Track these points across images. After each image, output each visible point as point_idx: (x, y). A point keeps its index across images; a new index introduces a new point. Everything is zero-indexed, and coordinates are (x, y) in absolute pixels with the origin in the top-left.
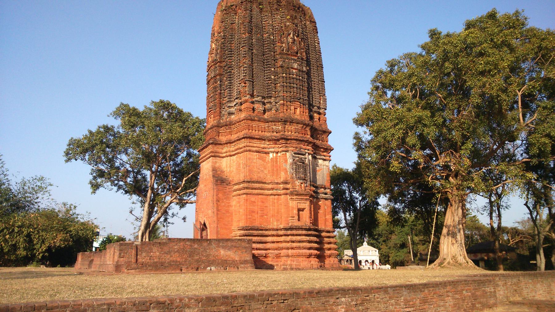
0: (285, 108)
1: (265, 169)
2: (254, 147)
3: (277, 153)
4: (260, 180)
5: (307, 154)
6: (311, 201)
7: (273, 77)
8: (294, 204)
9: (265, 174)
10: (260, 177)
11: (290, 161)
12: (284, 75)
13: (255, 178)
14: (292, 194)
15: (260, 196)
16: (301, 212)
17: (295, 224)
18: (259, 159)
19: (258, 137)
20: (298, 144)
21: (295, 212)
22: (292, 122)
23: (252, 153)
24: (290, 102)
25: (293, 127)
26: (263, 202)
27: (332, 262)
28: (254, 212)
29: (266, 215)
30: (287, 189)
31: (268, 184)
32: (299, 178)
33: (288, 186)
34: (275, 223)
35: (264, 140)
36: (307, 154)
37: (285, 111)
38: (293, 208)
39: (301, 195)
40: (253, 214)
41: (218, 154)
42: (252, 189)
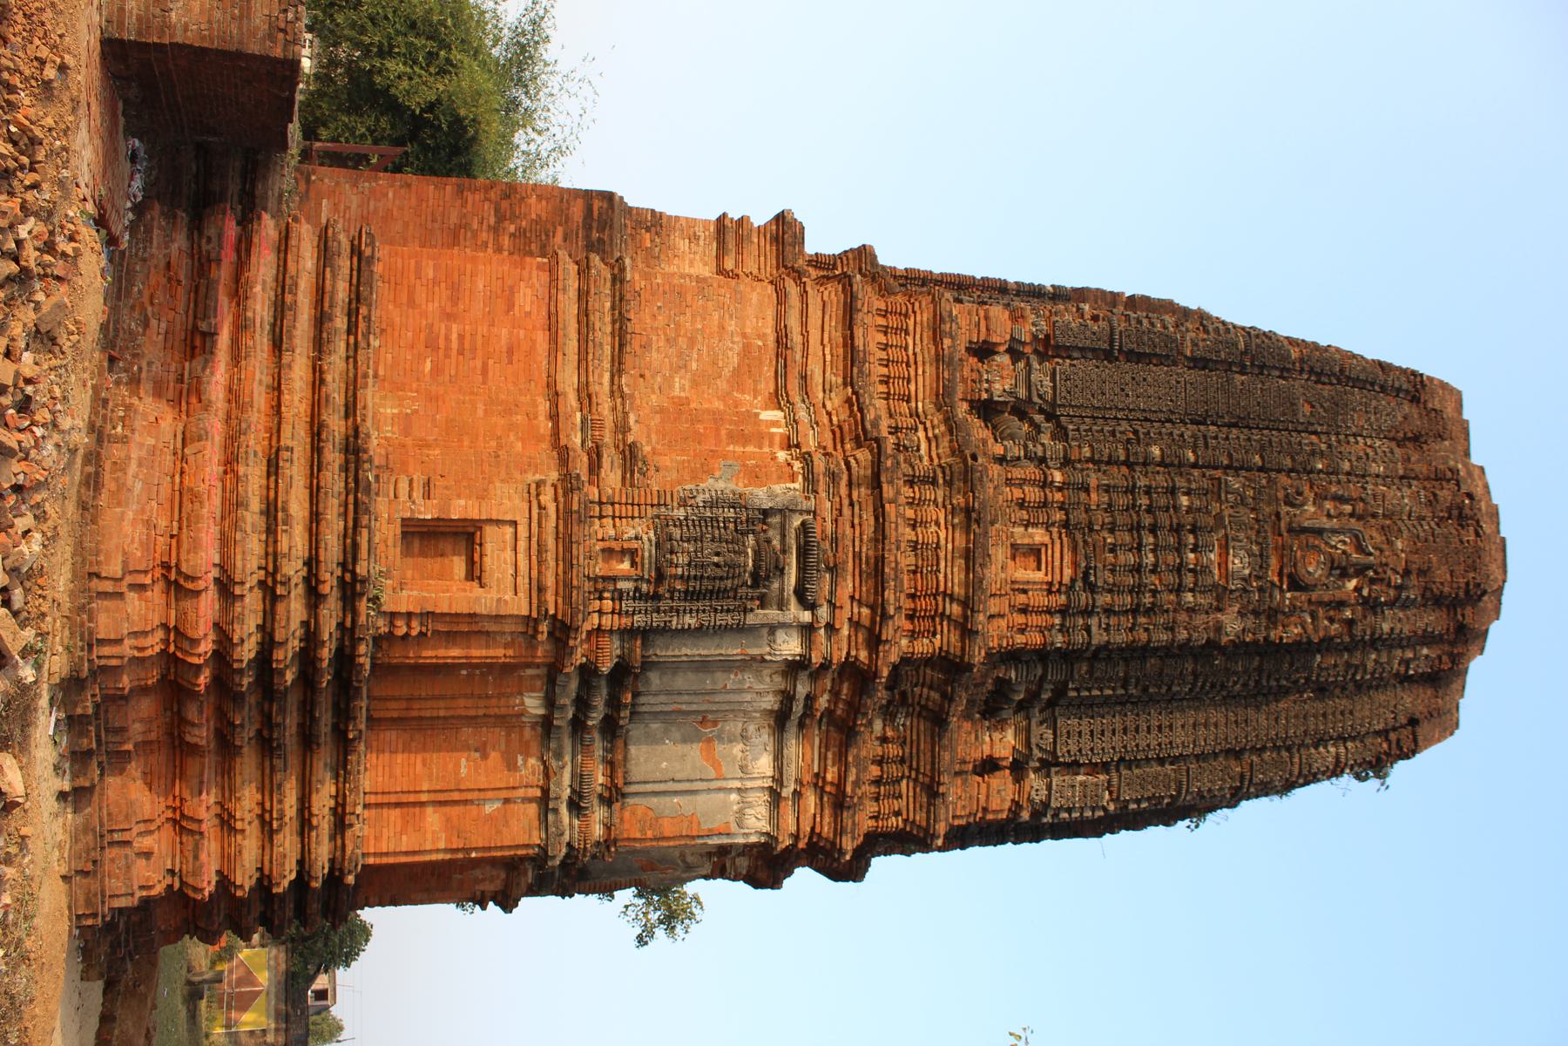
0: (1033, 494)
1: (695, 384)
2: (804, 324)
3: (789, 445)
4: (634, 344)
5: (806, 616)
6: (530, 622)
7: (1156, 451)
8: (507, 501)
9: (669, 381)
10: (646, 347)
11: (761, 496)
12: (1184, 501)
13: (642, 319)
14: (568, 484)
15: (541, 339)
16: (459, 565)
17: (381, 505)
18: (746, 350)
19: (859, 342)
20: (857, 556)
21: (461, 508)
22: (970, 517)
23: (770, 314)
24: (1066, 524)
25: (944, 534)
26: (510, 352)
27: (147, 842)
28: (455, 300)
29: (437, 371)
30: (595, 467)
31: (616, 391)
32: (664, 544)
33: (612, 476)
34: (390, 411)
35: (848, 381)
36: (806, 616)
37: (1018, 493)
38: (482, 496)
39: (566, 542)
40: (443, 292)
41: (731, 244)
42: (583, 295)
